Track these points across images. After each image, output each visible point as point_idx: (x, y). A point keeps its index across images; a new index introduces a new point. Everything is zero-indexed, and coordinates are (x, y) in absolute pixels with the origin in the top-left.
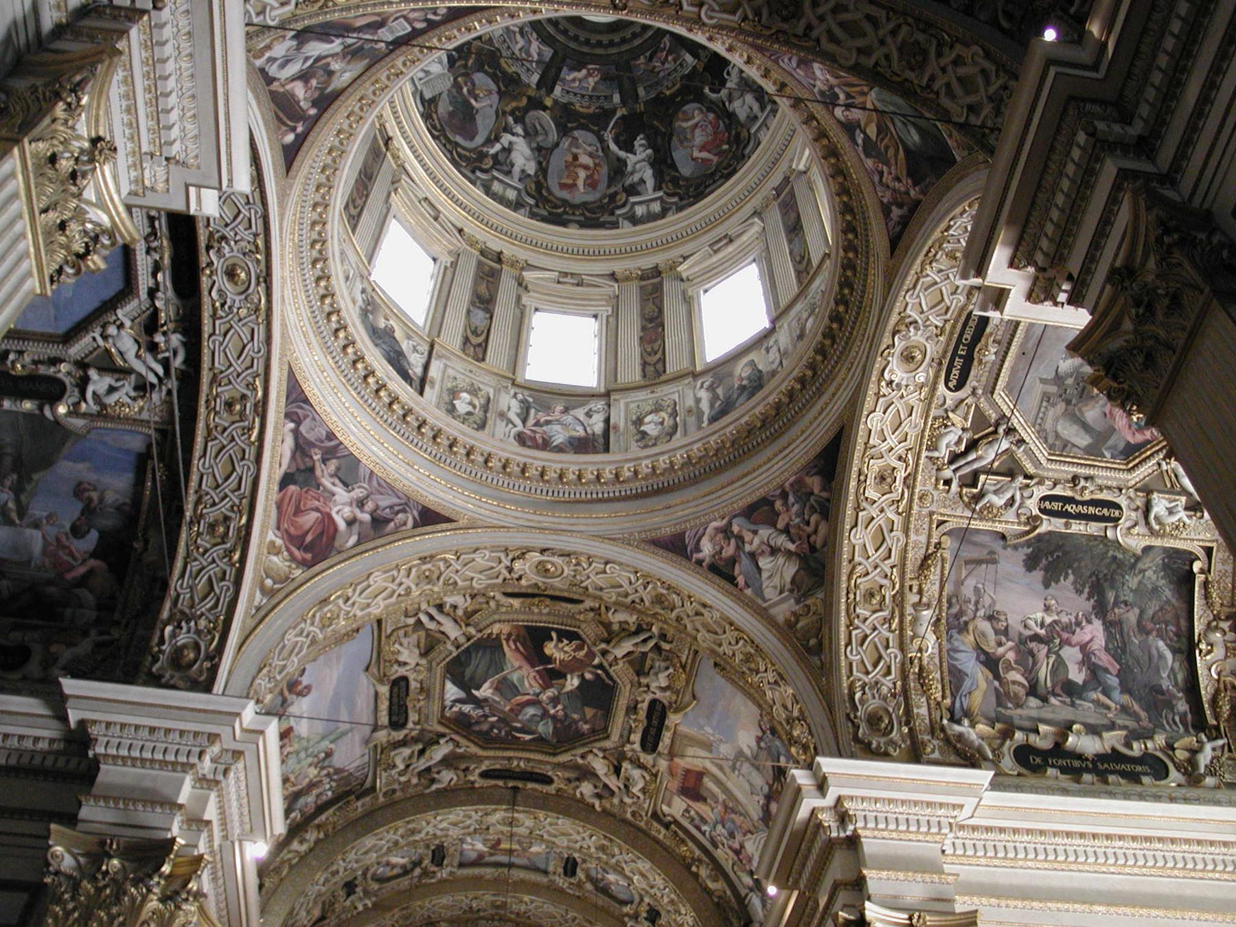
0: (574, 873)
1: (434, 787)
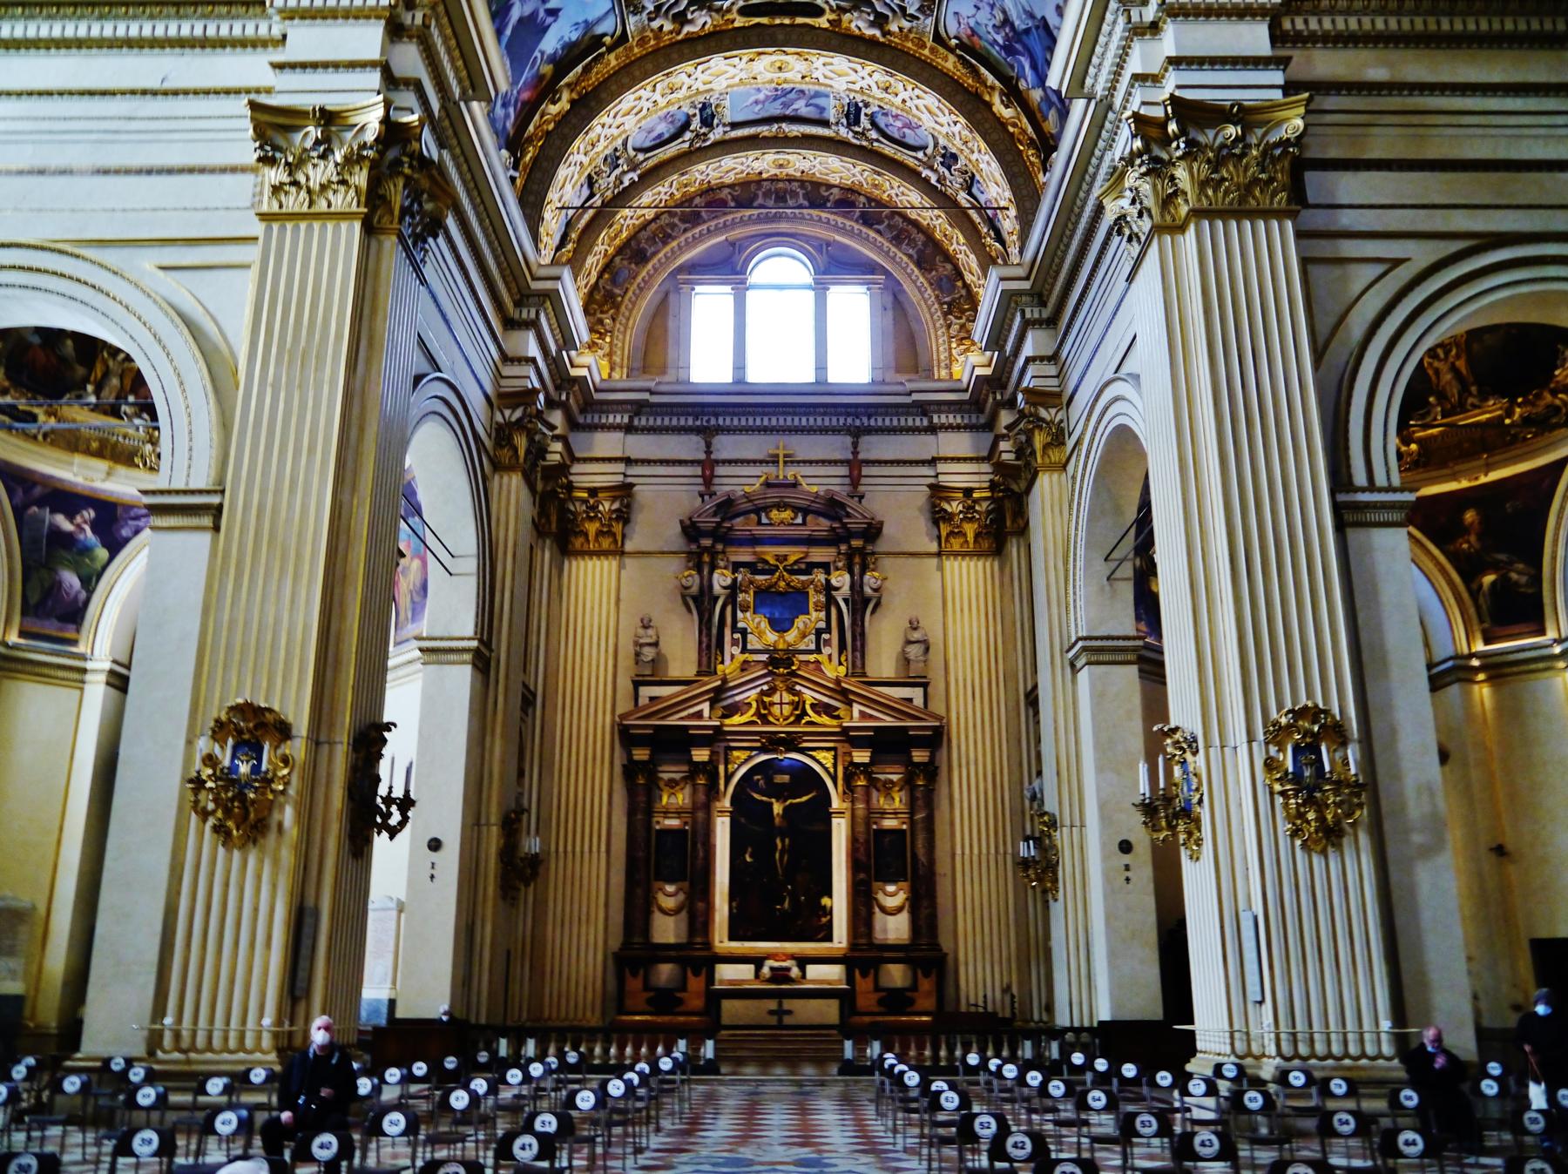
0: (857, 122)
1: (687, 29)
